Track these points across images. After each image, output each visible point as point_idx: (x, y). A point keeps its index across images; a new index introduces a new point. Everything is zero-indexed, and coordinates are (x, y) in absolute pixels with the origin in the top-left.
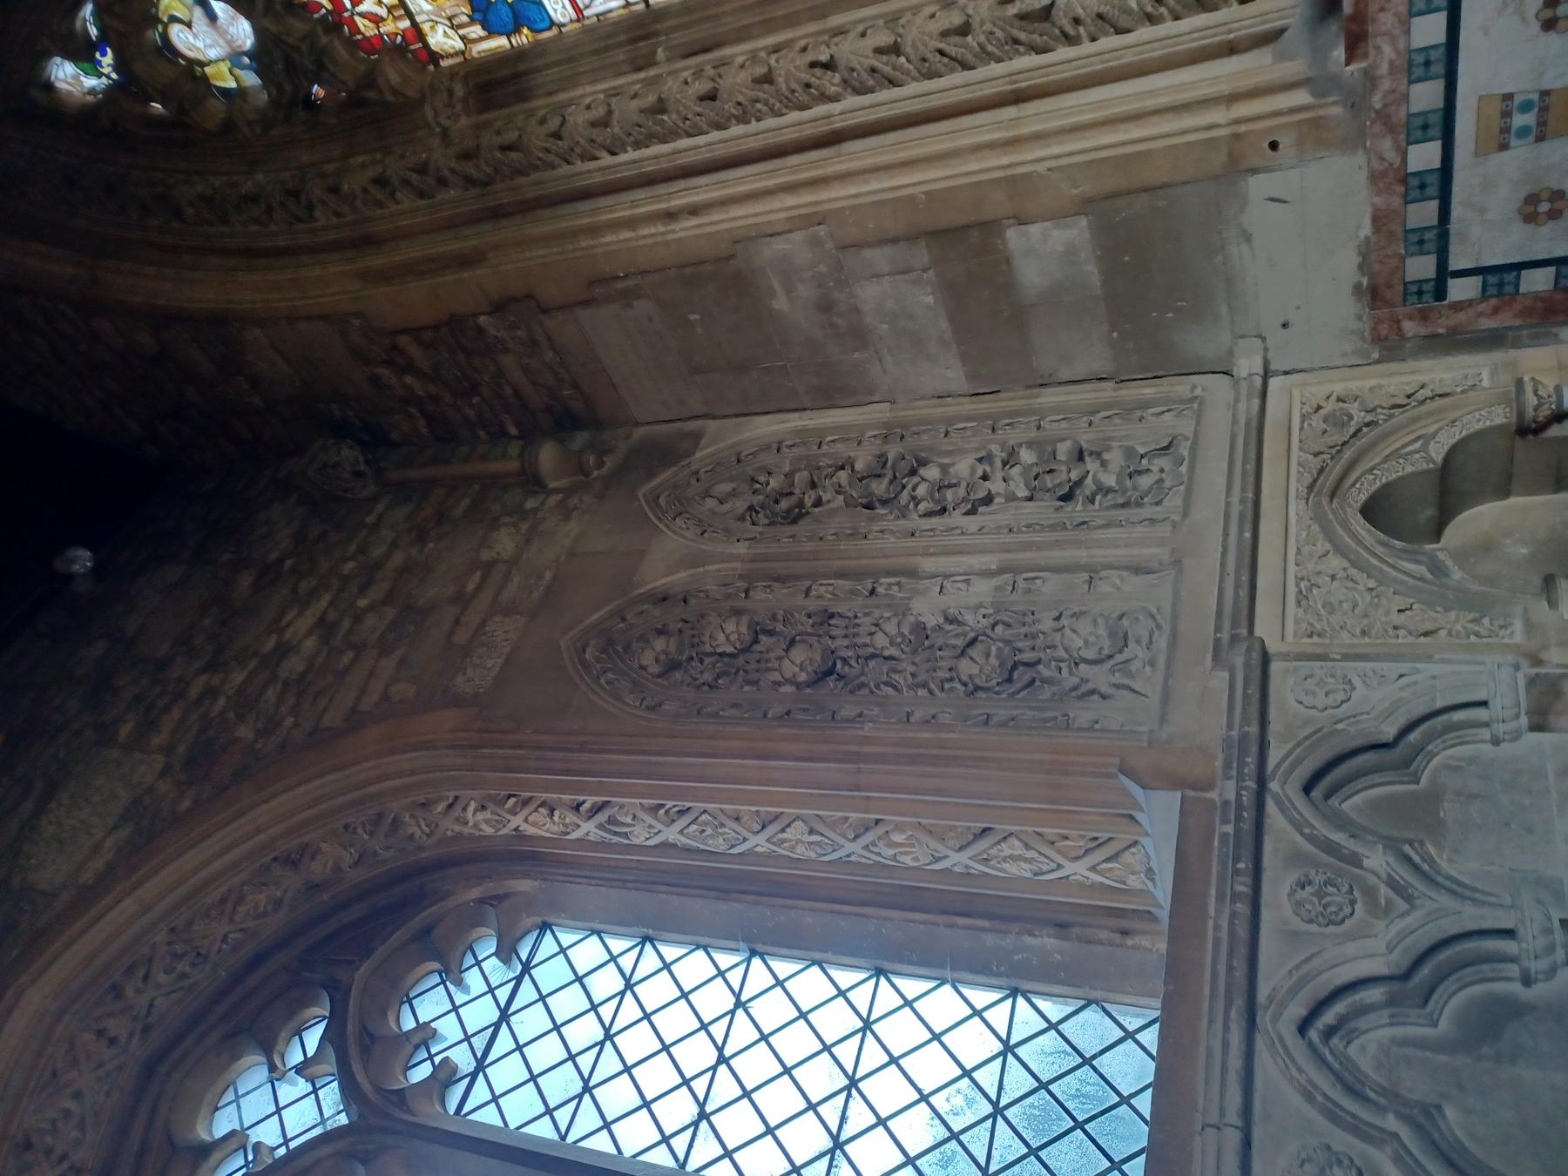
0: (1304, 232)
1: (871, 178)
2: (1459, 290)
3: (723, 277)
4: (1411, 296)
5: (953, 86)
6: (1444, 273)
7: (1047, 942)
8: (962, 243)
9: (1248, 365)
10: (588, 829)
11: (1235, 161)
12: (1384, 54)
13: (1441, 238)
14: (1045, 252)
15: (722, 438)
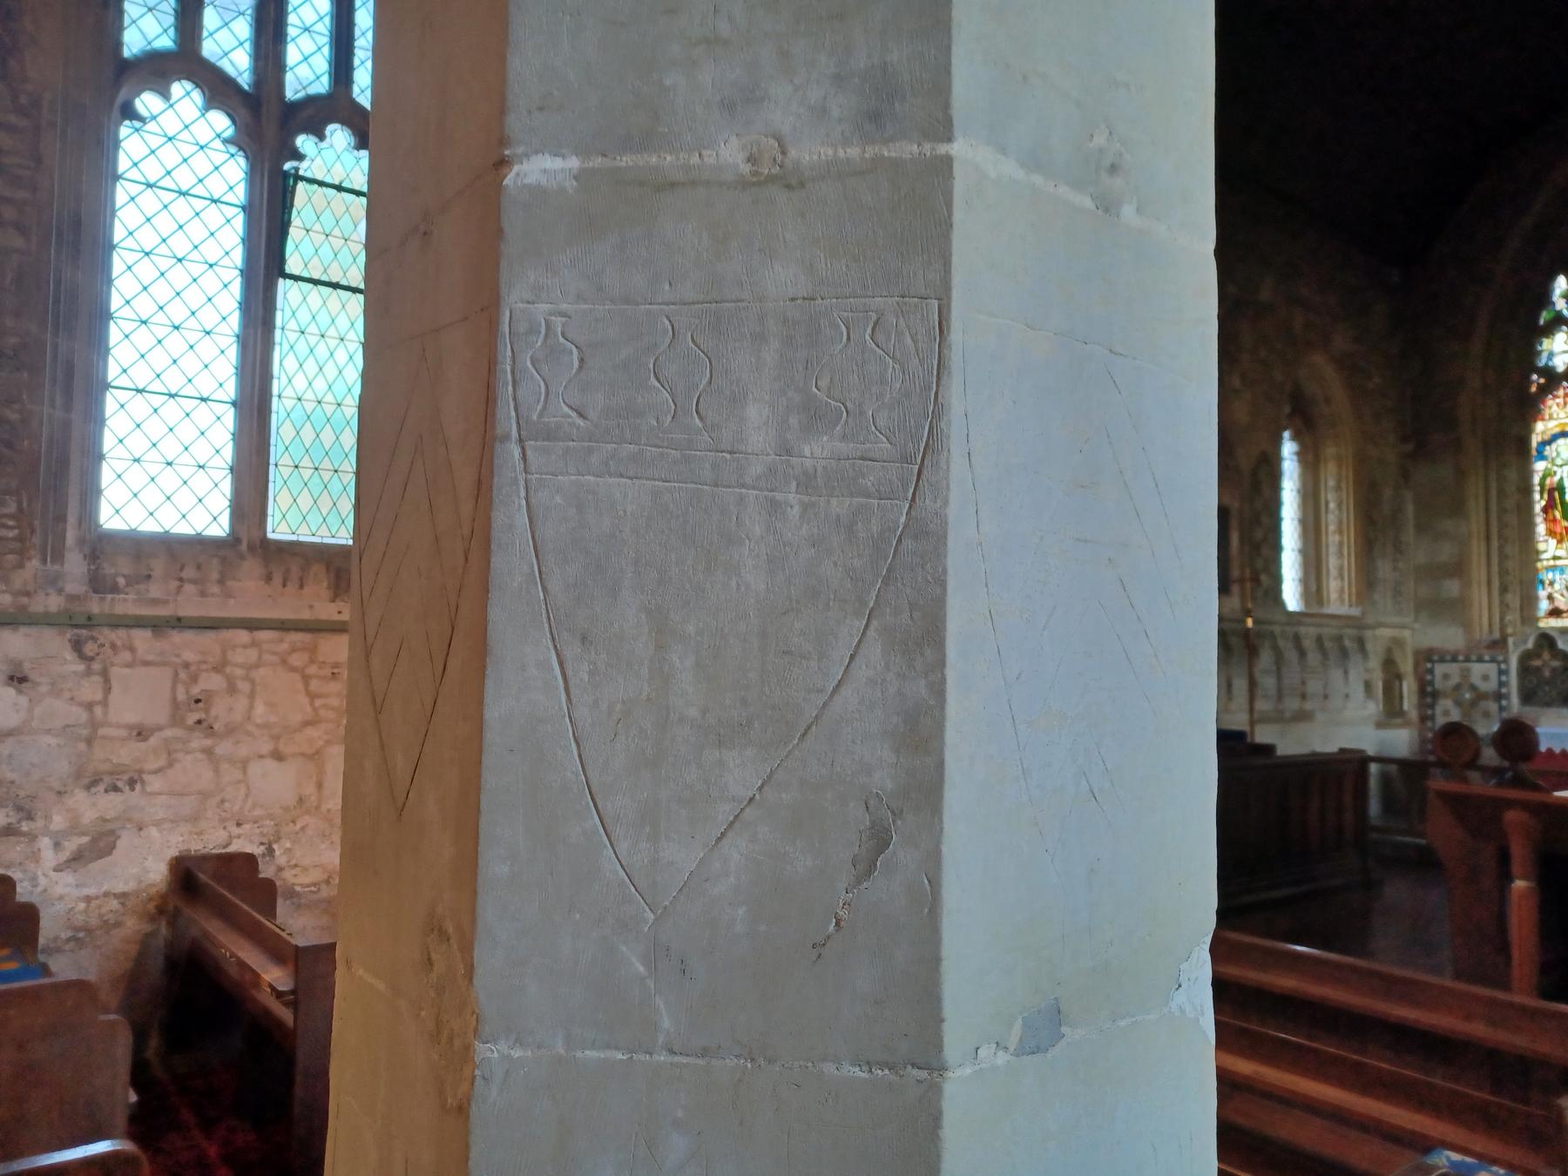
0: (1448, 636)
1: (1477, 550)
2: (1429, 665)
3: (1457, 508)
4: (1427, 657)
5: (1495, 568)
6: (1432, 662)
7: (1314, 588)
8: (1458, 569)
9: (1417, 626)
10: (1331, 483)
11: (1467, 626)
12: (1484, 651)
13: (1442, 660)
14: (1452, 587)
15: (1408, 496)
